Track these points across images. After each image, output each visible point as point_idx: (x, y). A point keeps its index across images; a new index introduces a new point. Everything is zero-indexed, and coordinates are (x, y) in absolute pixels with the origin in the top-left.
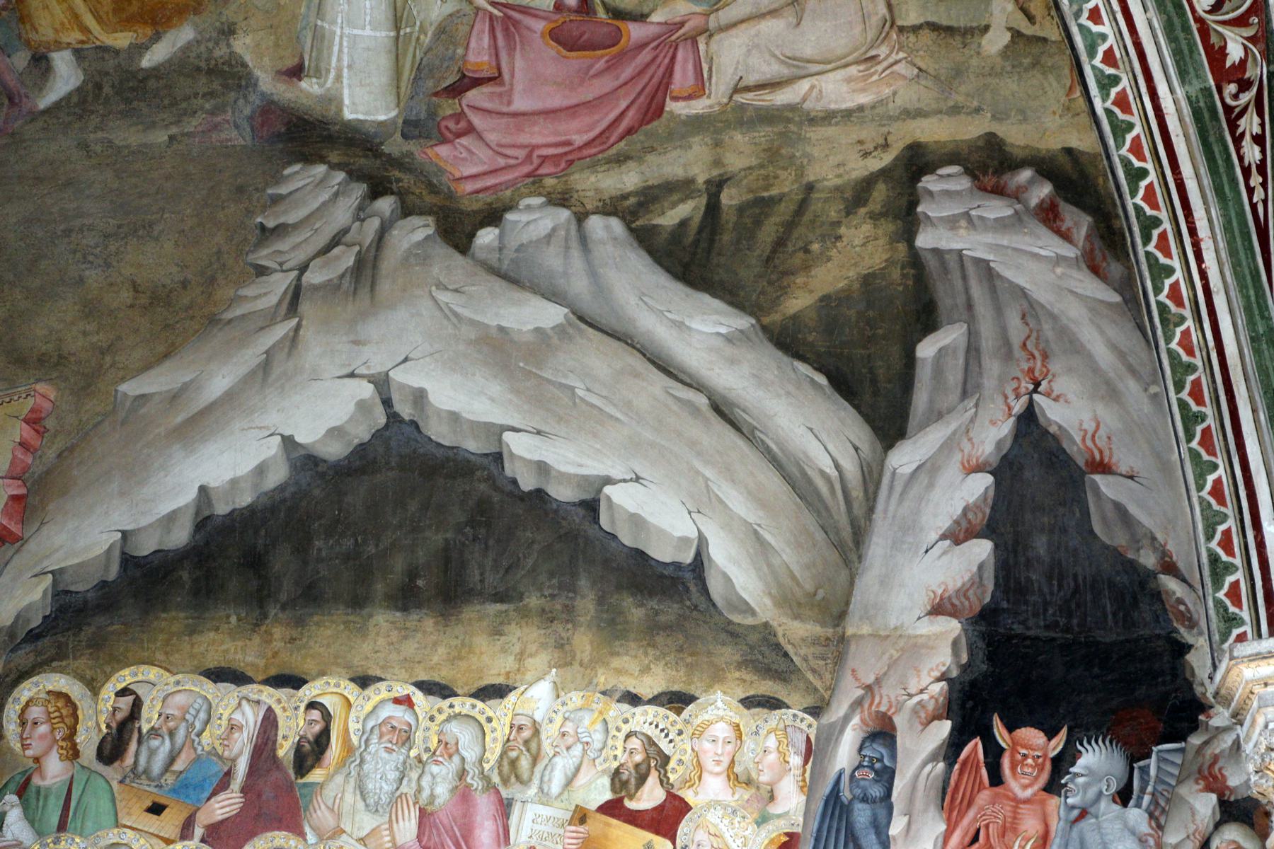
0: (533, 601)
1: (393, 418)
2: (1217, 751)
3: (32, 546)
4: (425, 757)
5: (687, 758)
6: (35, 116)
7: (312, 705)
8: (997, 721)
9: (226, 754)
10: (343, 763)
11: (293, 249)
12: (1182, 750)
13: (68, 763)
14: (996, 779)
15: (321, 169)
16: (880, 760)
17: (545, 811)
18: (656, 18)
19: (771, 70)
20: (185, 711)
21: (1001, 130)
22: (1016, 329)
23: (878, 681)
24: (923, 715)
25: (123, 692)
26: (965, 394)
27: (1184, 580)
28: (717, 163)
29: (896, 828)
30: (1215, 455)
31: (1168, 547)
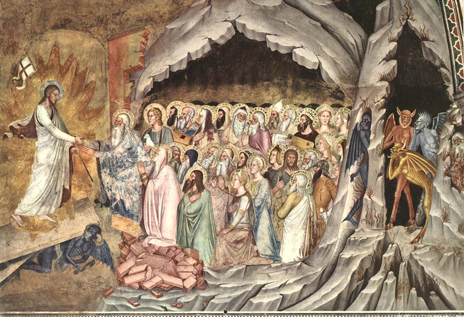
0: (276, 81)
1: (237, 31)
2: (454, 114)
3: (147, 70)
4: (250, 123)
5: (317, 121)
7: (220, 110)
8: (398, 108)
9: (199, 123)
10: (229, 125)
12: (445, 114)
13: (160, 126)
14: (398, 124)
16: (367, 120)
17: (282, 136)
23: (367, 99)
24: (378, 107)
25: (171, 108)
26: (389, 20)
27: (447, 69)
30: (457, 35)
31: (443, 60)
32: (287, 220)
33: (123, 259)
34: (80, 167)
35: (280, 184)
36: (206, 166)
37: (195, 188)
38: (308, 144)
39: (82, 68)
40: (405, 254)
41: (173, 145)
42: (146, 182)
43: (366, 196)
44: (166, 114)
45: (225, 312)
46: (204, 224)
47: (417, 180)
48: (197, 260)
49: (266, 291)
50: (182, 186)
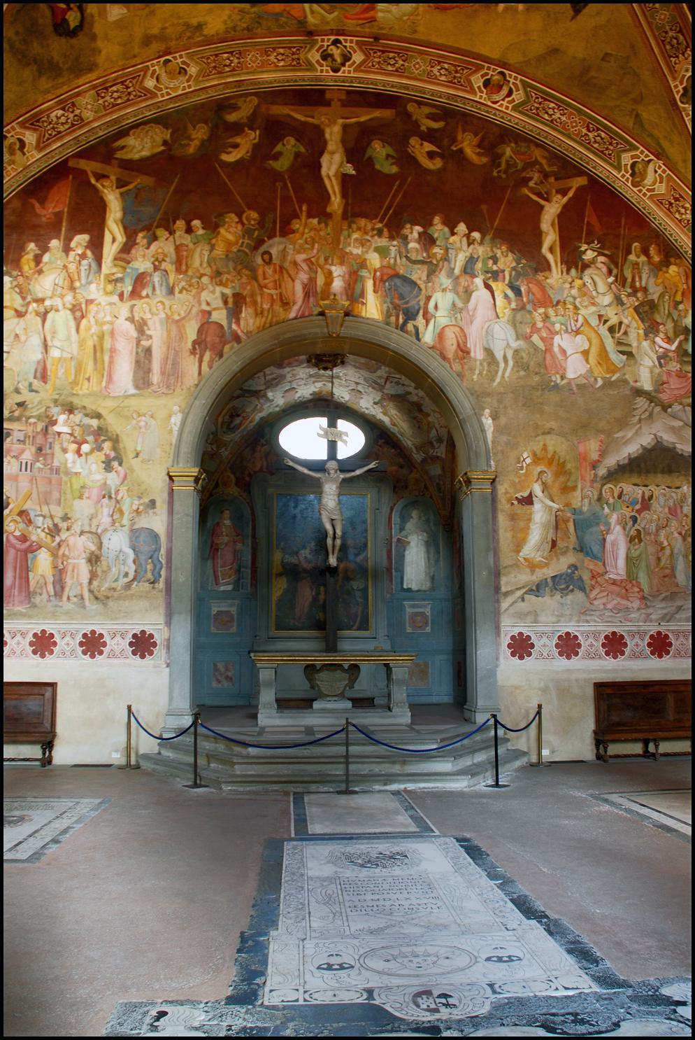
0: (683, 472)
33: (593, 587)
34: (562, 525)
39: (562, 461)
46: (643, 564)
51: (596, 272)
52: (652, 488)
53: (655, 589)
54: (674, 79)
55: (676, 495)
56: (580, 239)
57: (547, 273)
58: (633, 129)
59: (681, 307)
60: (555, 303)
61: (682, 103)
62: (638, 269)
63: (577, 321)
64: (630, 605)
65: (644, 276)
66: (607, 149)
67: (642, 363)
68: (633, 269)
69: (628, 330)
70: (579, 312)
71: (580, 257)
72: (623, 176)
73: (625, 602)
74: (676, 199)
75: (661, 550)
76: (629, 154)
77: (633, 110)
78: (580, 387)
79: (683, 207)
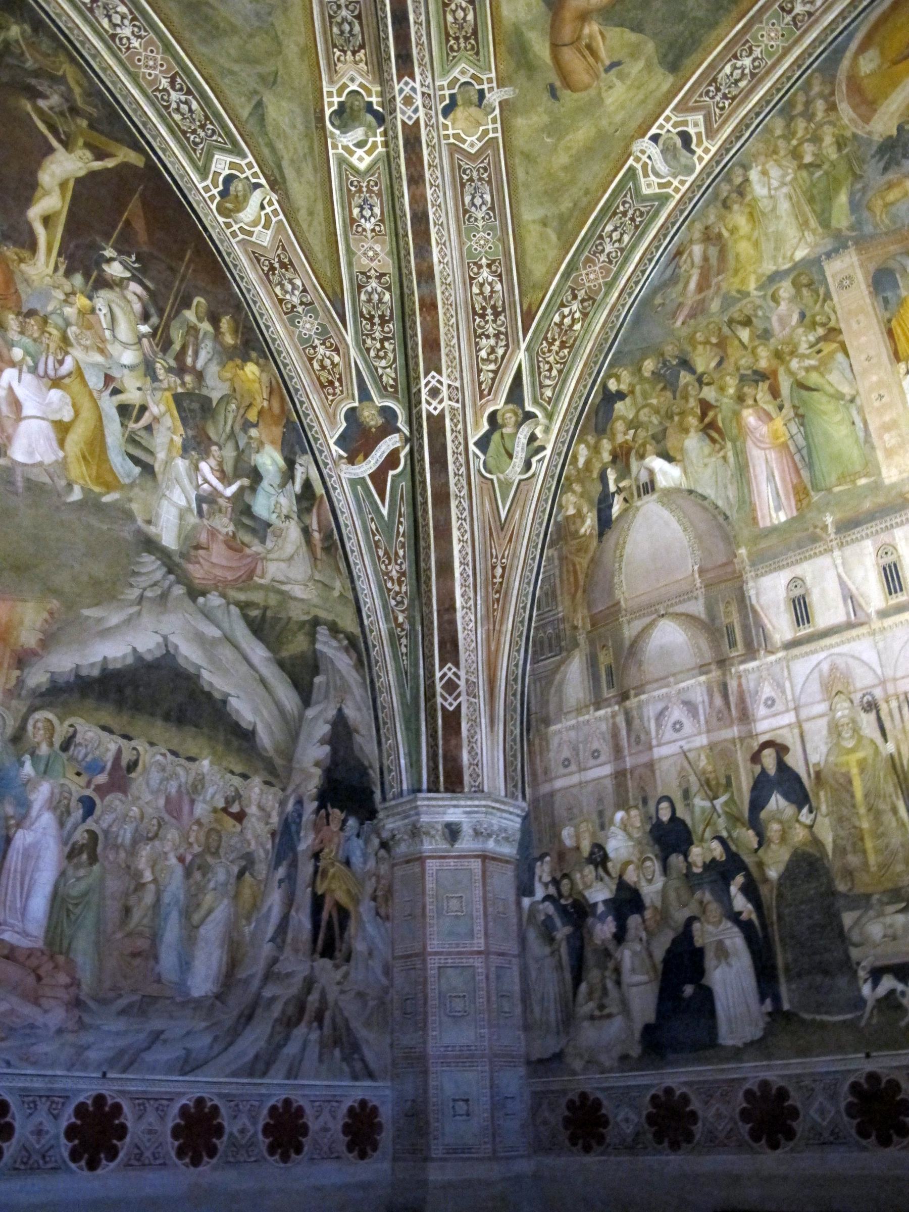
1: (168, 651)
6: (65, 504)
7: (134, 749)
10: (141, 774)
11: (143, 581)
14: (328, 824)
15: (153, 558)
17: (205, 806)
18: (254, 549)
19: (282, 578)
20: (92, 738)
21: (338, 620)
22: (339, 682)
25: (71, 726)
28: (266, 601)
29: (302, 834)
32: (202, 930)
35: (197, 875)
36: (105, 825)
37: (84, 857)
38: (234, 826)
40: (331, 998)
41: (62, 781)
42: (13, 831)
43: (293, 913)
44: (62, 731)
45: (104, 1074)
46: (89, 920)
47: (344, 900)
48: (73, 978)
49: (165, 1041)
50: (67, 849)
51: (118, 300)
52: (141, 745)
53: (107, 984)
54: (331, 82)
55: (184, 774)
56: (107, 236)
57: (25, 254)
58: (246, 121)
59: (253, 432)
60: (25, 310)
61: (333, 124)
62: (197, 338)
63: (61, 362)
64: (40, 1020)
65: (203, 356)
66: (194, 132)
67: (167, 493)
68: (187, 333)
69: (155, 426)
70: (69, 349)
71: (98, 265)
72: (207, 189)
73: (28, 1010)
74: (283, 265)
75: (136, 890)
76: (229, 159)
77: (256, 92)
78: (32, 486)
79: (291, 281)
